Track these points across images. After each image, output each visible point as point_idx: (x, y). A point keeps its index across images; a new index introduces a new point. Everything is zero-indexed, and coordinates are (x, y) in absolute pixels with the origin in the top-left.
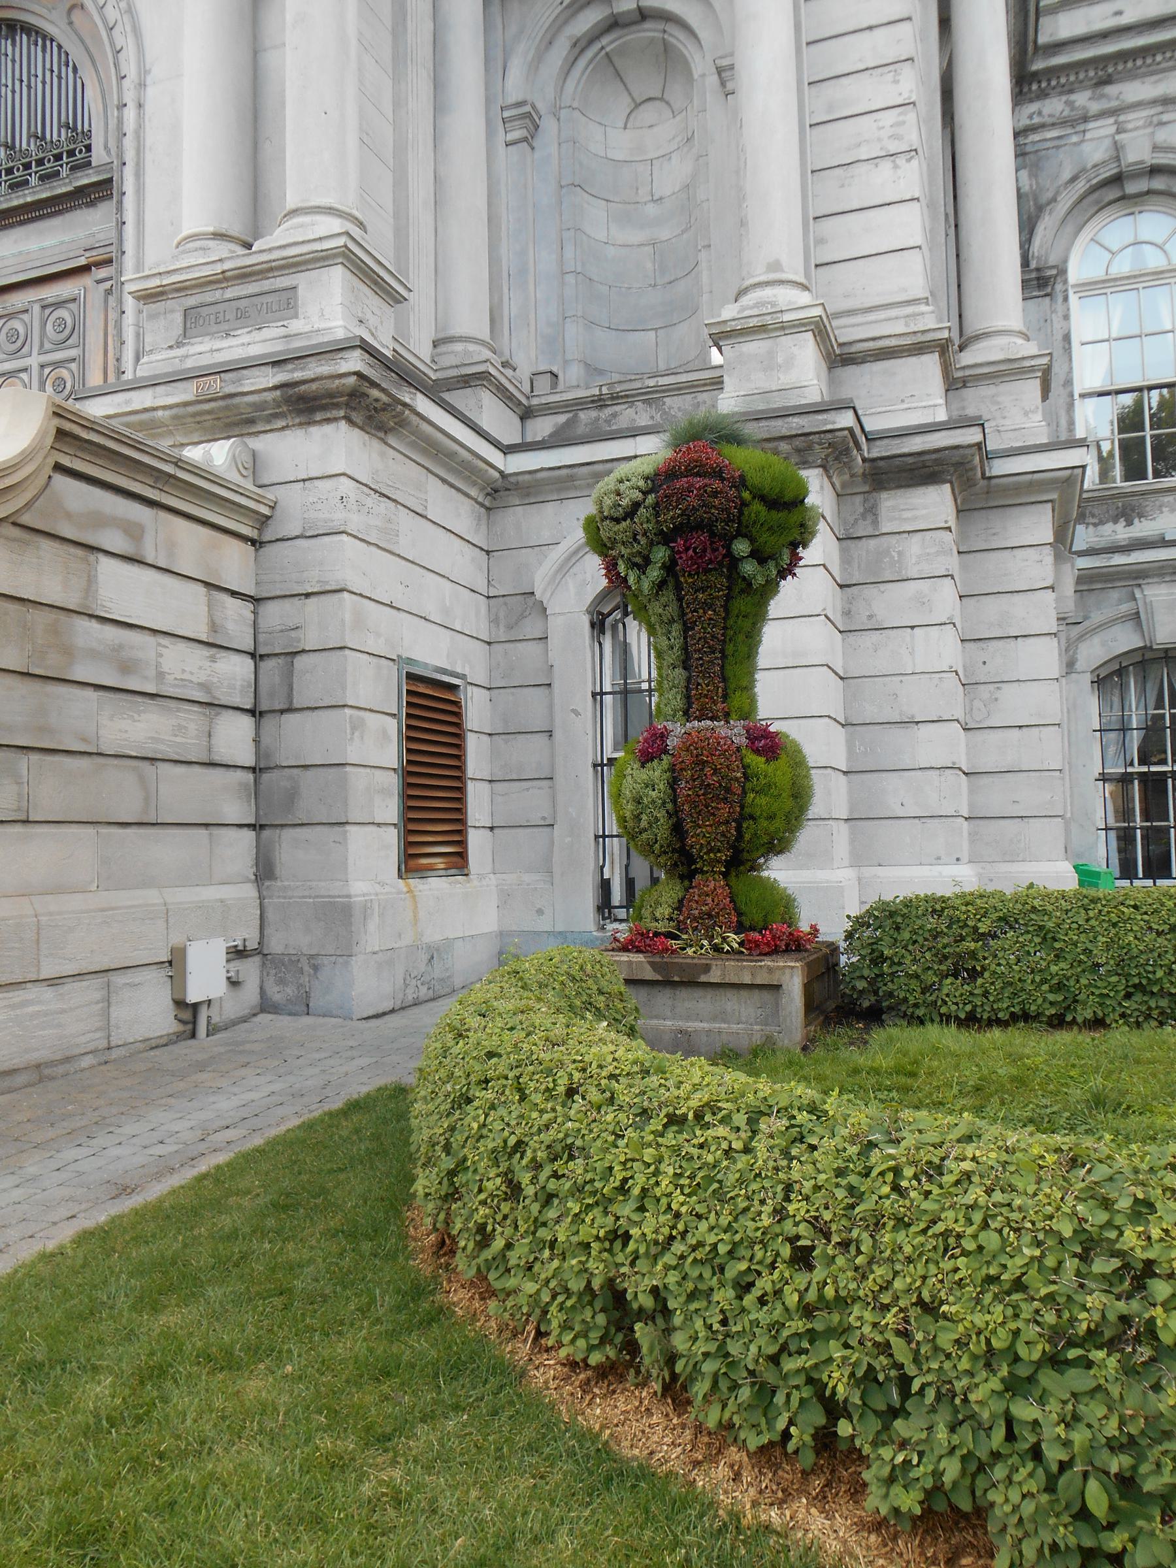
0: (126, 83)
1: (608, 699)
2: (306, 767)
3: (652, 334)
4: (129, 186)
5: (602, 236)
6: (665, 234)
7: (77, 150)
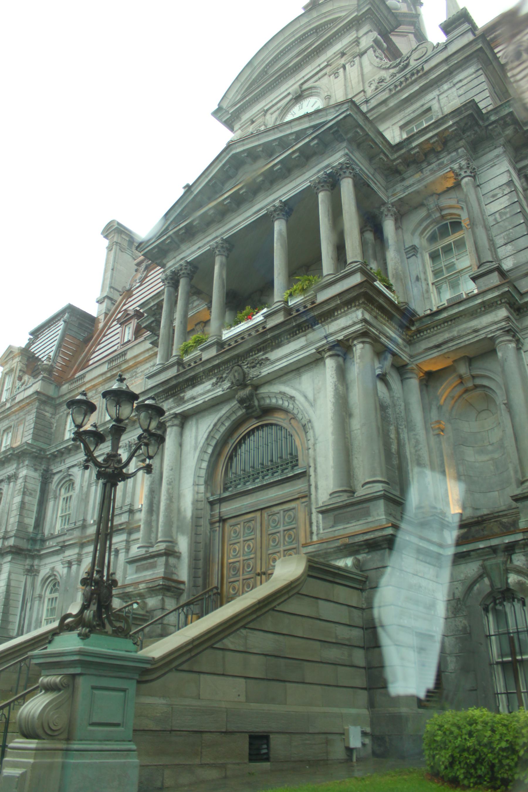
0: (309, 442)
1: (493, 638)
3: (497, 493)
5: (472, 459)
6: (496, 456)
7: (294, 461)
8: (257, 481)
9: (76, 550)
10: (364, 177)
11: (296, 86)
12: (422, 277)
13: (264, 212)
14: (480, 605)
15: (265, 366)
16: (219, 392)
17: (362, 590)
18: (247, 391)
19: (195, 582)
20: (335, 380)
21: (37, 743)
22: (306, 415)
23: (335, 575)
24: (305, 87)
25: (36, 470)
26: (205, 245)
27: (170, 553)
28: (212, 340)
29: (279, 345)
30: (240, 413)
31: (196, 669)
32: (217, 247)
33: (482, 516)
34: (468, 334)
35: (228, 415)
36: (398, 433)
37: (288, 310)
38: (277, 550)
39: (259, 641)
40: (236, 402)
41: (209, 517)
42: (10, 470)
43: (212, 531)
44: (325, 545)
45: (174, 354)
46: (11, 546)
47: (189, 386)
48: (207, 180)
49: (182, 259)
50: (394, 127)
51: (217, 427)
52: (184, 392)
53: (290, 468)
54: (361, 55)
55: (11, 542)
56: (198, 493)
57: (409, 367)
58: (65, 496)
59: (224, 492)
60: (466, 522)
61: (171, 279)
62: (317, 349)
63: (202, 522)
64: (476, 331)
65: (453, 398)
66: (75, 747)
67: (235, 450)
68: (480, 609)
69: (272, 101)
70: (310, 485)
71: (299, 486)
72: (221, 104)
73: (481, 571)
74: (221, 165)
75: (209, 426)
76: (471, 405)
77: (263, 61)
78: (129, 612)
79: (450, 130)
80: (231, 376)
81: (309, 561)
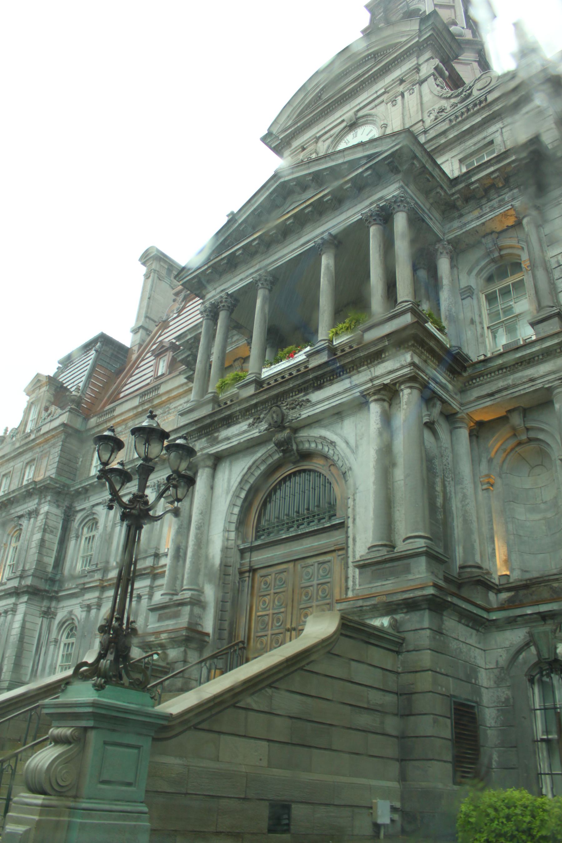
1: (538, 712)
2: (417, 737)
4: (350, 524)
5: (523, 518)
6: (549, 515)
8: (291, 529)
9: (97, 594)
10: (420, 212)
11: (351, 113)
12: (477, 319)
13: (311, 245)
14: (526, 675)
15: (306, 408)
16: (255, 433)
17: (398, 653)
18: (286, 433)
19: (220, 634)
20: (379, 426)
21: (44, 799)
22: (347, 462)
23: (370, 635)
24: (360, 114)
25: (58, 506)
26: (247, 277)
27: (197, 602)
28: (250, 377)
29: (320, 387)
30: (276, 457)
31: (216, 728)
32: (260, 280)
33: (530, 580)
34: (524, 383)
35: (264, 458)
36: (444, 486)
37: (332, 350)
38: (309, 605)
39: (285, 701)
40: (273, 445)
41: (238, 566)
42: (31, 505)
43: (242, 580)
44: (360, 603)
45: (210, 391)
46: (27, 586)
47: (224, 425)
48: (252, 209)
49: (222, 291)
50: (453, 160)
51: (252, 471)
52: (218, 431)
53: (327, 517)
54: (421, 83)
55: (28, 581)
56: (228, 539)
57: (459, 416)
58: (88, 536)
59: (256, 539)
60: (513, 585)
61: (210, 311)
62: (361, 392)
63: (230, 570)
64: (532, 380)
65: (505, 450)
66: (84, 805)
67: (269, 496)
68: (525, 679)
69: (324, 128)
70: (347, 537)
71: (336, 537)
72: (272, 129)
73: (528, 639)
74: (268, 193)
75: (244, 469)
76: (524, 458)
77: (317, 85)
78: (148, 663)
79: (513, 166)
80: (269, 417)
81: (342, 618)
